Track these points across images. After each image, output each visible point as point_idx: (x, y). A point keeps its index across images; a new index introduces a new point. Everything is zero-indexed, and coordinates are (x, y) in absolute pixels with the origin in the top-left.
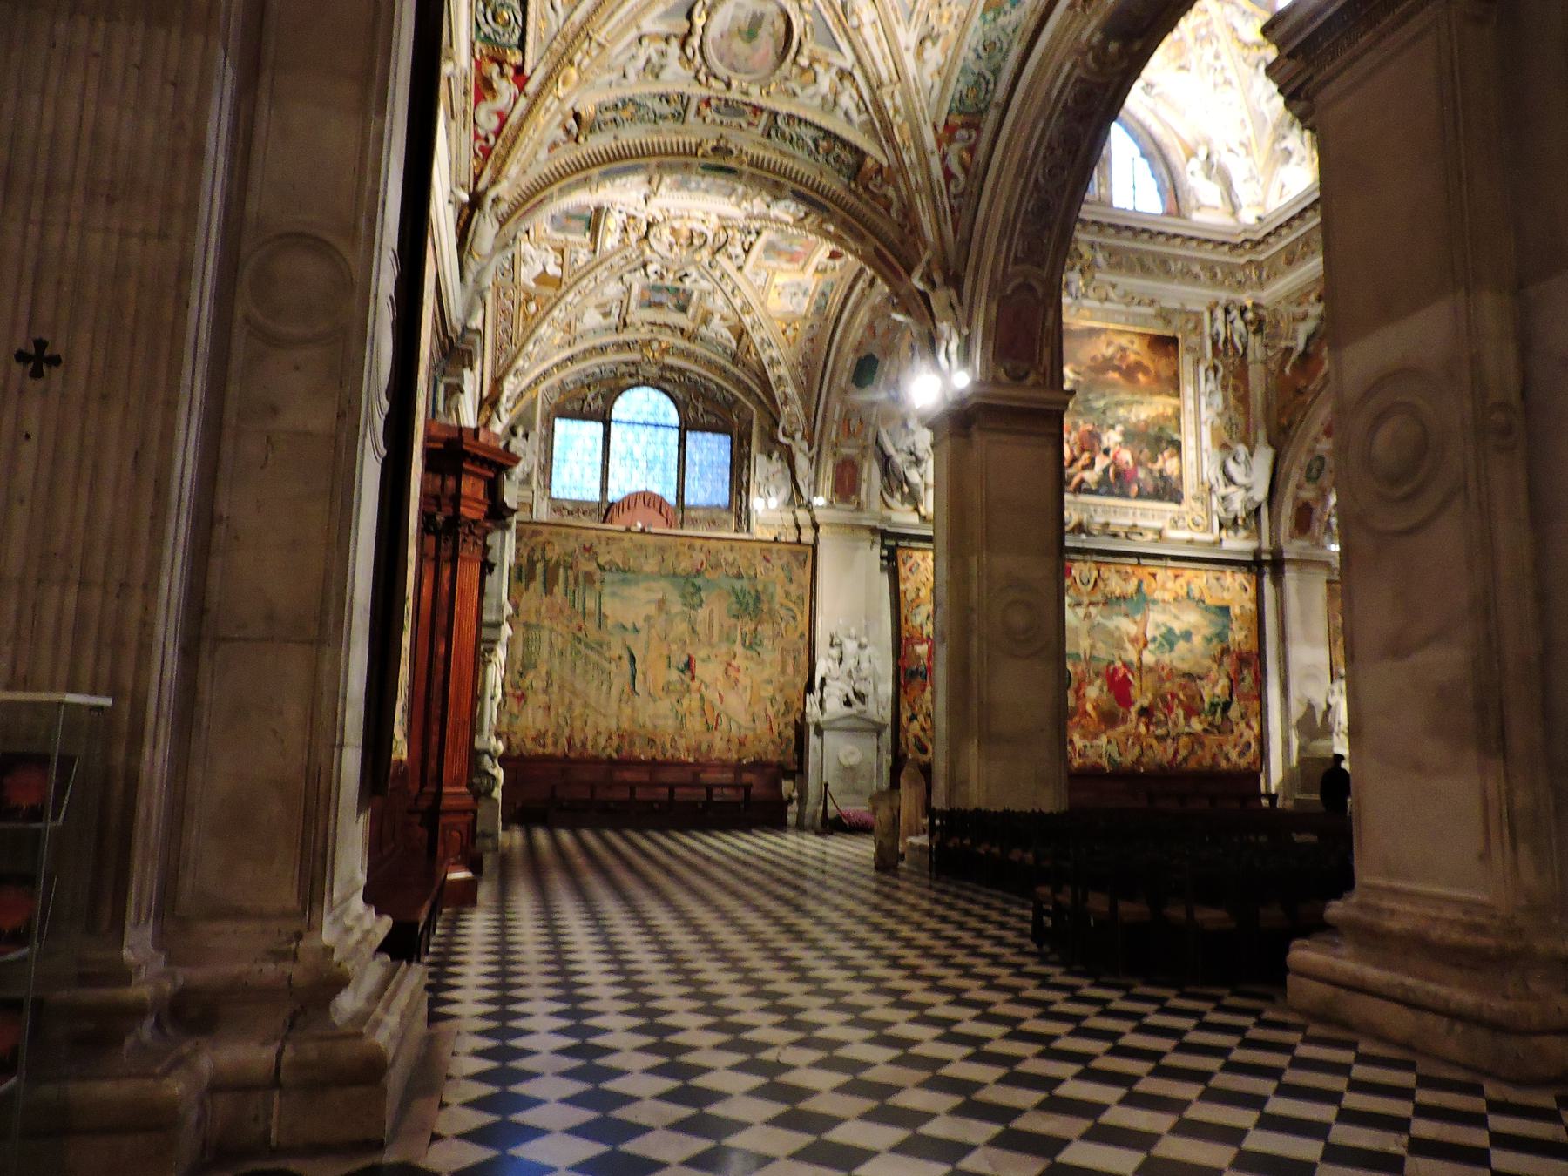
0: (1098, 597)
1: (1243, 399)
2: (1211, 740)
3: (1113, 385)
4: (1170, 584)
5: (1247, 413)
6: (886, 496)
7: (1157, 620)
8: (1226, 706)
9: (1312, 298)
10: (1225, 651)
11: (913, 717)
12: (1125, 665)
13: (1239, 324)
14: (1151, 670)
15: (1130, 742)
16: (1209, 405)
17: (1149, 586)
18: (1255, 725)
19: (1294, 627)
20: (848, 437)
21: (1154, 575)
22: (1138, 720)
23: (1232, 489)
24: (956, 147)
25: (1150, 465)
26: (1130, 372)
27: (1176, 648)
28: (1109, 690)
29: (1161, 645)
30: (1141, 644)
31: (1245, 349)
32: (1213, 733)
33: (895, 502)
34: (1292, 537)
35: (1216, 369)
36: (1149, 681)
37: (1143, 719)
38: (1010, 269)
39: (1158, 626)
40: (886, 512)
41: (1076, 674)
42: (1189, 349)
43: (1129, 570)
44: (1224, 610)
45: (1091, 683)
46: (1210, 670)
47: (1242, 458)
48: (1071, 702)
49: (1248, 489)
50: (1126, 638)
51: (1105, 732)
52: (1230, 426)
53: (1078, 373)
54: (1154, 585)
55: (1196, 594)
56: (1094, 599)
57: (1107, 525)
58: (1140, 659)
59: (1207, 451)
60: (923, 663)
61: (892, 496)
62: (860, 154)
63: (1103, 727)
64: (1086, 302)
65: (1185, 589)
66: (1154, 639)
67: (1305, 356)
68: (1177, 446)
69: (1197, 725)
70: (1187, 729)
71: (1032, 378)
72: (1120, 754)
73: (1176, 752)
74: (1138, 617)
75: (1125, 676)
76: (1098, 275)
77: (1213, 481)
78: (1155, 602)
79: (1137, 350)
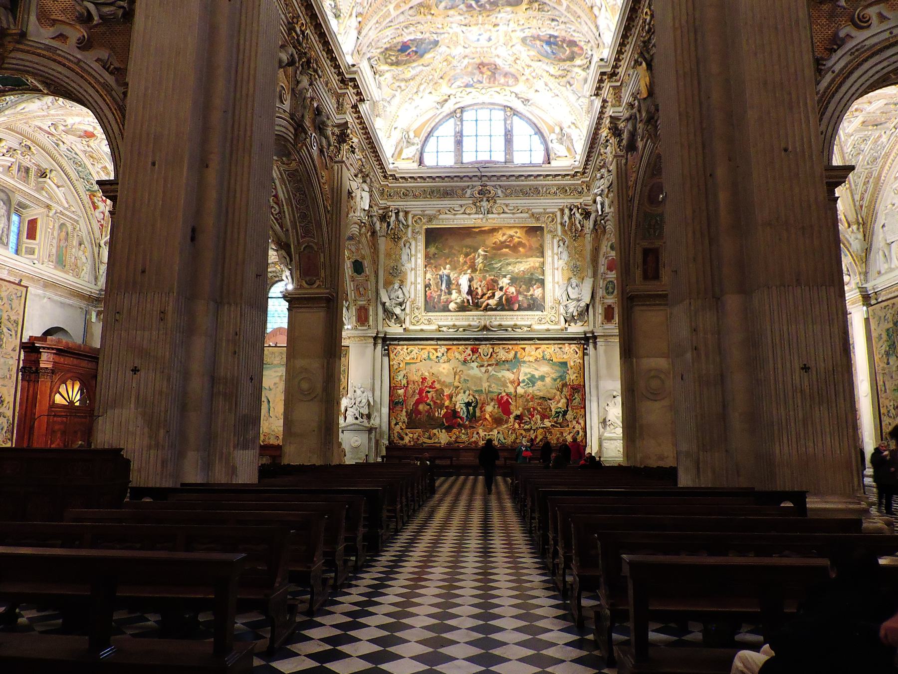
1: (580, 253)
2: (555, 431)
3: (505, 255)
4: (533, 353)
7: (525, 371)
8: (565, 413)
10: (565, 385)
11: (396, 424)
12: (507, 395)
13: (578, 215)
15: (510, 433)
21: (524, 349)
28: (499, 407)
30: (516, 384)
31: (582, 226)
32: (557, 427)
36: (520, 401)
37: (517, 421)
39: (526, 374)
41: (481, 400)
43: (510, 347)
46: (555, 394)
48: (478, 414)
51: (496, 428)
54: (524, 354)
56: (490, 363)
57: (500, 325)
58: (516, 391)
59: (558, 283)
61: (391, 321)
63: (495, 426)
64: (490, 216)
65: (542, 354)
66: (524, 381)
68: (542, 283)
69: (547, 423)
70: (542, 426)
73: (536, 437)
74: (515, 371)
76: (498, 202)
78: (524, 362)
79: (519, 235)
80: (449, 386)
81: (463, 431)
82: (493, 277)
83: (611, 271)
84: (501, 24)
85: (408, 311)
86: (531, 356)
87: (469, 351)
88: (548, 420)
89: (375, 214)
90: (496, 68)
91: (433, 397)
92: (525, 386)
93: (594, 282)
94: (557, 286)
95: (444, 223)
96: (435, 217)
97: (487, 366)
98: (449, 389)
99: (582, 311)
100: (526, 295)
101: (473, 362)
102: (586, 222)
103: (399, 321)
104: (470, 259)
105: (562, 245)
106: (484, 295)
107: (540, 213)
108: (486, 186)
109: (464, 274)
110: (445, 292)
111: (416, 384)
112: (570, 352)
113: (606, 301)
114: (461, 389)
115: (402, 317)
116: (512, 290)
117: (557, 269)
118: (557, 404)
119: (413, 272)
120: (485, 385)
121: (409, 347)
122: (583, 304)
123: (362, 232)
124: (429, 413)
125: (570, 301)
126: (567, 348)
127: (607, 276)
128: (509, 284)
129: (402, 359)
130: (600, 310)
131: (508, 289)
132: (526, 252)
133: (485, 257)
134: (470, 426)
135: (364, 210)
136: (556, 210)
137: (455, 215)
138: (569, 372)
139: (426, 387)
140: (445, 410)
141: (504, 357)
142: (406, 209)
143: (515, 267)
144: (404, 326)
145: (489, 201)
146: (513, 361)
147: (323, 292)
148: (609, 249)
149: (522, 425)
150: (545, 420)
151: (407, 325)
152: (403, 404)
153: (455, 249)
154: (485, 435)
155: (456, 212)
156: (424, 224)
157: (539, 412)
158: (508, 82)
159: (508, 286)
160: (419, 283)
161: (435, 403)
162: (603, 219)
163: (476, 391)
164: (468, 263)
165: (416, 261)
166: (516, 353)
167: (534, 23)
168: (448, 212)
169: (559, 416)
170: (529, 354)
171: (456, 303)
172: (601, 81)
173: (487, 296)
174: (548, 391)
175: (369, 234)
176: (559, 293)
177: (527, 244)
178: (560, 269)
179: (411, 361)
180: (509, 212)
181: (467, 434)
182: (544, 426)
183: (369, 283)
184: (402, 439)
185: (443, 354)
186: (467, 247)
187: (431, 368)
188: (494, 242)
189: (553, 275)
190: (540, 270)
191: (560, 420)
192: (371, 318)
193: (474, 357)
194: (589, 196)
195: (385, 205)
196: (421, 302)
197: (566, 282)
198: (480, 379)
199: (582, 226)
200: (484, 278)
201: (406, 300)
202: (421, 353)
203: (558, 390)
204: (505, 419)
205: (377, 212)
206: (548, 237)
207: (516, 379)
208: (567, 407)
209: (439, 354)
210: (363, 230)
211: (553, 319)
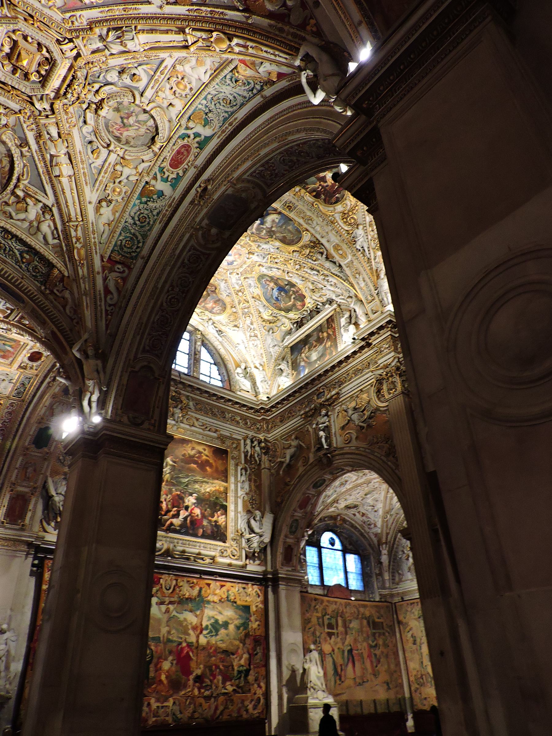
1: (259, 487)
4: (218, 591)
5: (260, 495)
6: (45, 524)
8: (247, 672)
9: (293, 437)
10: (247, 635)
12: (189, 645)
13: (257, 449)
14: (204, 648)
15: (188, 703)
17: (206, 591)
18: (263, 684)
19: (284, 620)
21: (209, 585)
22: (194, 686)
23: (253, 535)
24: (114, 275)
26: (203, 465)
27: (219, 633)
28: (177, 664)
29: (211, 632)
34: (282, 565)
35: (246, 471)
36: (202, 656)
37: (197, 684)
38: (139, 356)
39: (210, 618)
40: (42, 534)
41: (156, 652)
43: (195, 581)
44: (246, 608)
45: (166, 659)
47: (258, 518)
48: (152, 674)
49: (261, 536)
50: (190, 627)
52: (252, 501)
55: (232, 598)
56: (172, 599)
58: (197, 641)
62: (51, 266)
63: (171, 692)
64: (182, 425)
65: (226, 594)
66: (207, 627)
67: (289, 465)
68: (225, 508)
71: (146, 425)
72: (181, 713)
73: (216, 708)
74: (198, 613)
76: (189, 413)
77: (243, 530)
78: (208, 602)
84: (256, 254)
86: (215, 594)
90: (214, 292)
92: (208, 634)
97: (168, 604)
105: (244, 473)
107: (227, 437)
108: (180, 394)
126: (250, 589)
133: (173, 468)
136: (240, 438)
141: (188, 594)
146: (197, 599)
149: (202, 691)
154: (158, 707)
157: (221, 673)
158: (213, 308)
166: (201, 589)
167: (290, 267)
169: (240, 677)
170: (214, 592)
172: (381, 328)
177: (214, 464)
180: (198, 426)
182: (226, 691)
203: (241, 642)
204: (183, 681)
207: (199, 625)
208: (249, 665)
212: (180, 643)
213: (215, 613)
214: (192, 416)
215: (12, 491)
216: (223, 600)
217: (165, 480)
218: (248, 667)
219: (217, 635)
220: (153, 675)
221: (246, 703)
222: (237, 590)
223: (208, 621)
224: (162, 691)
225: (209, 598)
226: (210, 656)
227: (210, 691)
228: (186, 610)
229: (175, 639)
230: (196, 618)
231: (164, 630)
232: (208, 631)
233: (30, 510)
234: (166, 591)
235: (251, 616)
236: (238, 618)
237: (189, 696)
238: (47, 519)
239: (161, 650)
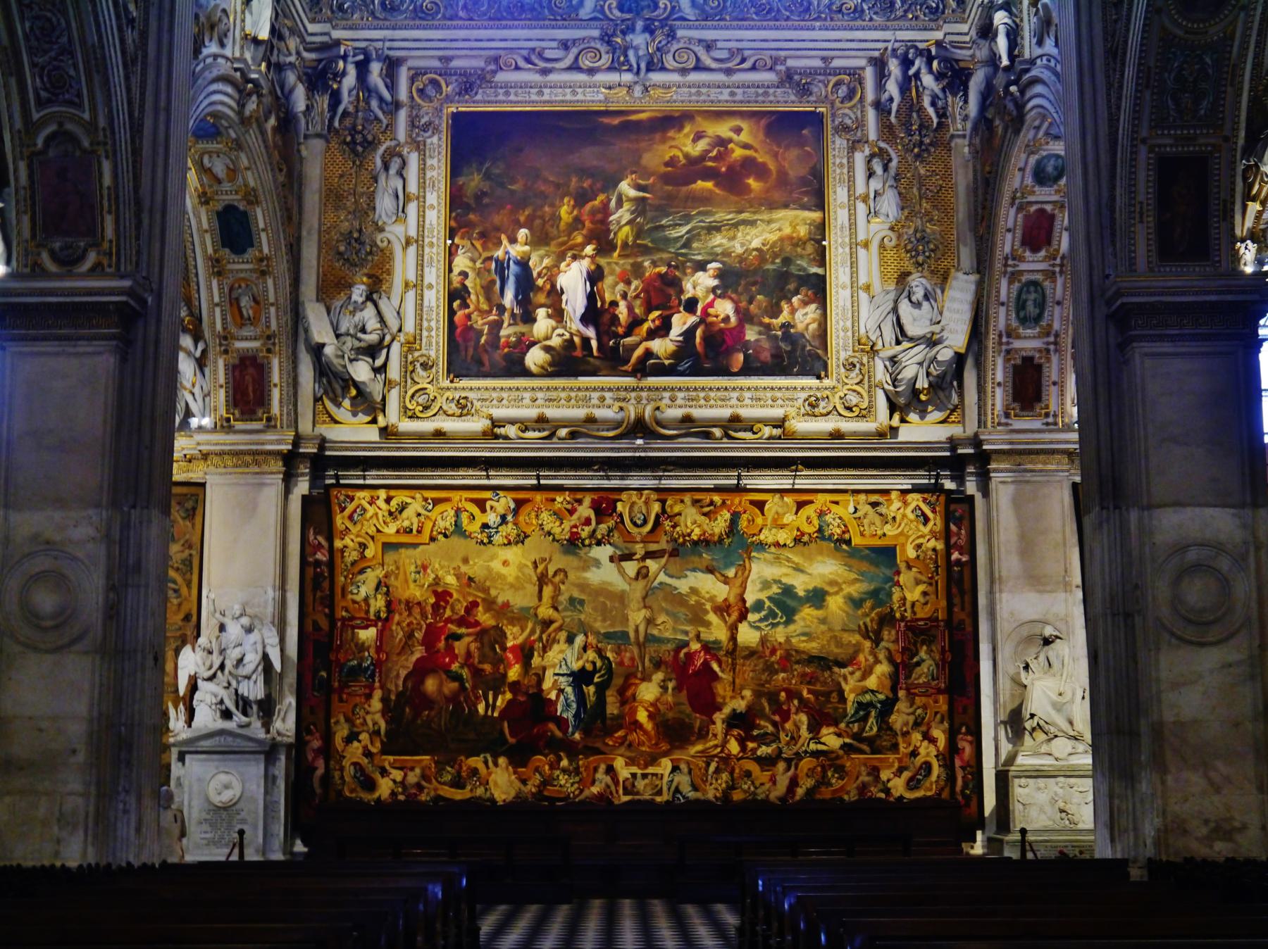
0: (663, 544)
3: (705, 199)
4: (788, 518)
8: (888, 707)
10: (887, 620)
11: (352, 737)
12: (707, 647)
13: (928, 80)
14: (752, 653)
15: (712, 768)
16: (872, 213)
17: (751, 521)
20: (242, 326)
21: (760, 505)
25: (767, 320)
27: (796, 618)
28: (678, 689)
30: (735, 616)
32: (862, 752)
33: (343, 413)
36: (748, 671)
39: (766, 585)
41: (621, 663)
42: (843, 129)
43: (717, 498)
44: (885, 555)
45: (646, 678)
48: (612, 708)
50: (708, 606)
51: (665, 754)
53: (639, 188)
56: (653, 547)
57: (687, 419)
58: (733, 638)
59: (867, 288)
60: (369, 656)
61: (339, 405)
63: (664, 746)
64: (656, 77)
65: (816, 522)
66: (759, 606)
68: (818, 289)
69: (830, 739)
70: (813, 746)
72: (695, 788)
73: (794, 783)
74: (731, 573)
75: (706, 664)
76: (680, 33)
78: (761, 546)
80: (519, 619)
81: (565, 763)
82: (663, 269)
83: (1035, 250)
85: (394, 372)
86: (782, 527)
87: (585, 510)
88: (832, 730)
89: (292, 59)
91: (469, 654)
92: (761, 620)
93: (980, 285)
94: (863, 296)
95: (512, 98)
96: (482, 78)
97: (643, 559)
98: (523, 630)
99: (942, 377)
100: (768, 327)
101: (599, 543)
102: (955, 103)
103: (369, 405)
104: (593, 212)
105: (878, 169)
106: (635, 323)
107: (813, 72)
109: (575, 258)
110: (513, 315)
111: (416, 611)
112: (904, 516)
113: (1017, 344)
114: (560, 629)
115: (376, 390)
116: (725, 308)
117: (866, 245)
118: (864, 678)
119: (412, 250)
120: (637, 617)
121: (392, 493)
122: (945, 355)
123: (247, 113)
124: (457, 705)
125: (906, 345)
126: (897, 504)
127: (1023, 267)
128: (714, 290)
129: (372, 531)
130: (998, 371)
131: (711, 305)
132: (767, 191)
134: (586, 747)
135: (256, 41)
136: (863, 63)
137: (545, 72)
138: (902, 579)
139: (449, 620)
140: (509, 696)
141: (697, 531)
142: (392, 53)
143: (733, 238)
144: (382, 421)
145: (652, 32)
146: (727, 541)
147: (111, 287)
148: (1029, 181)
149: (751, 745)
150: (824, 731)
151: (392, 416)
152: (372, 676)
153: (546, 181)
154: (634, 775)
155: (549, 65)
156: (449, 99)
157: (803, 705)
159: (712, 296)
160: (430, 286)
161: (477, 673)
162: (1015, 83)
163: (608, 636)
164: (587, 224)
165: (421, 216)
166: (735, 517)
168: (522, 63)
170: (775, 520)
171: (548, 349)
173: (646, 326)
174: (835, 637)
175: (272, 121)
176: (871, 318)
177: (772, 166)
178: (874, 246)
179: (404, 539)
180: (714, 65)
181: (577, 771)
182: (820, 747)
183: (270, 282)
184: (371, 785)
185: (503, 517)
186: (584, 172)
187: (466, 561)
188: (667, 158)
189: (854, 265)
190: (810, 248)
191: (872, 728)
192: (276, 394)
193: (603, 528)
194: (964, 21)
195: (325, 39)
196: (435, 346)
197: (892, 287)
198: (621, 598)
199: (942, 114)
200: (637, 270)
201: (388, 338)
202: (433, 515)
205: (298, 53)
206: (837, 146)
207: (732, 600)
208: (894, 689)
209: (492, 518)
210: (252, 105)
211: (853, 399)
212: (686, 644)
213: (785, 570)
214: (690, 39)
215: (226, 352)
216: (806, 538)
217: (619, 243)
218: (891, 695)
219: (789, 621)
220: (615, 712)
221: (884, 775)
222: (851, 509)
223: (761, 590)
224: (641, 744)
225: (762, 537)
226: (770, 669)
227: (774, 746)
228: (694, 570)
229: (668, 635)
230: (727, 587)
231: (637, 617)
232: (763, 613)
233: (275, 385)
234: (634, 530)
235: (898, 573)
236: (856, 580)
237: (715, 756)
238: (331, 395)
239: (632, 659)
